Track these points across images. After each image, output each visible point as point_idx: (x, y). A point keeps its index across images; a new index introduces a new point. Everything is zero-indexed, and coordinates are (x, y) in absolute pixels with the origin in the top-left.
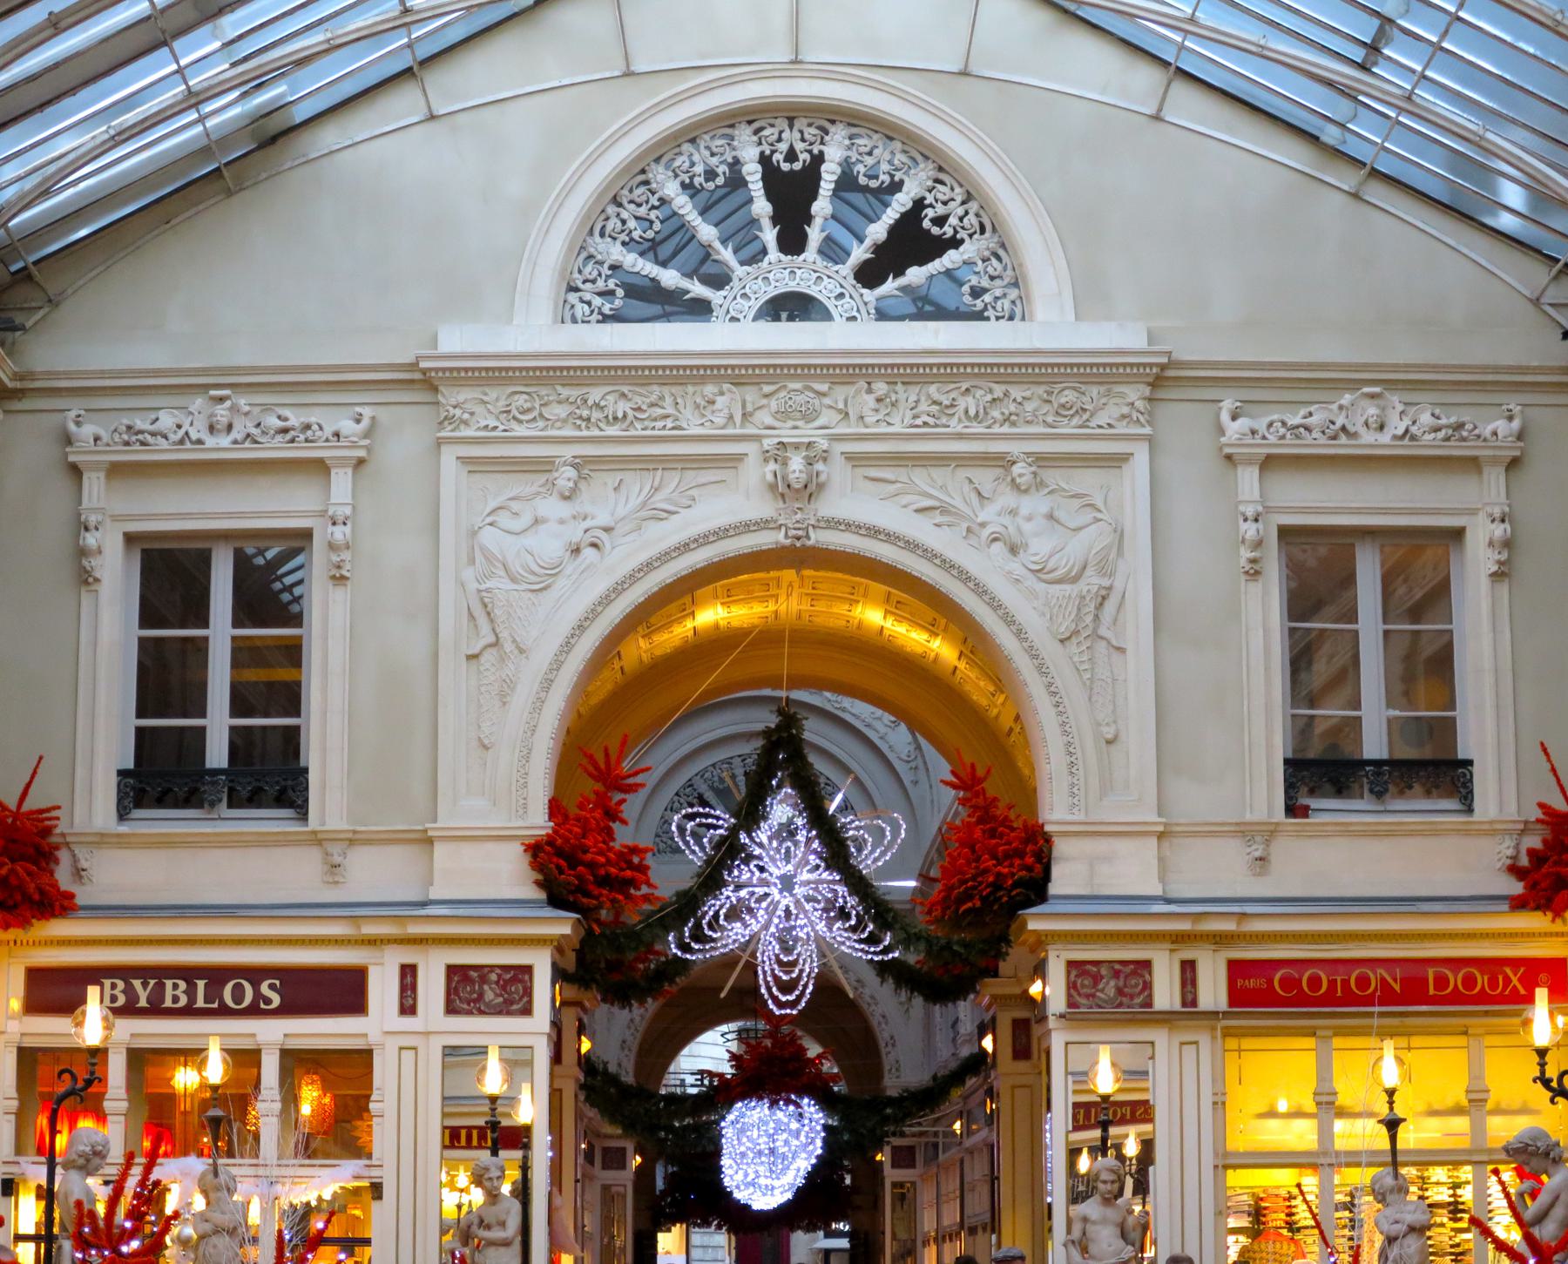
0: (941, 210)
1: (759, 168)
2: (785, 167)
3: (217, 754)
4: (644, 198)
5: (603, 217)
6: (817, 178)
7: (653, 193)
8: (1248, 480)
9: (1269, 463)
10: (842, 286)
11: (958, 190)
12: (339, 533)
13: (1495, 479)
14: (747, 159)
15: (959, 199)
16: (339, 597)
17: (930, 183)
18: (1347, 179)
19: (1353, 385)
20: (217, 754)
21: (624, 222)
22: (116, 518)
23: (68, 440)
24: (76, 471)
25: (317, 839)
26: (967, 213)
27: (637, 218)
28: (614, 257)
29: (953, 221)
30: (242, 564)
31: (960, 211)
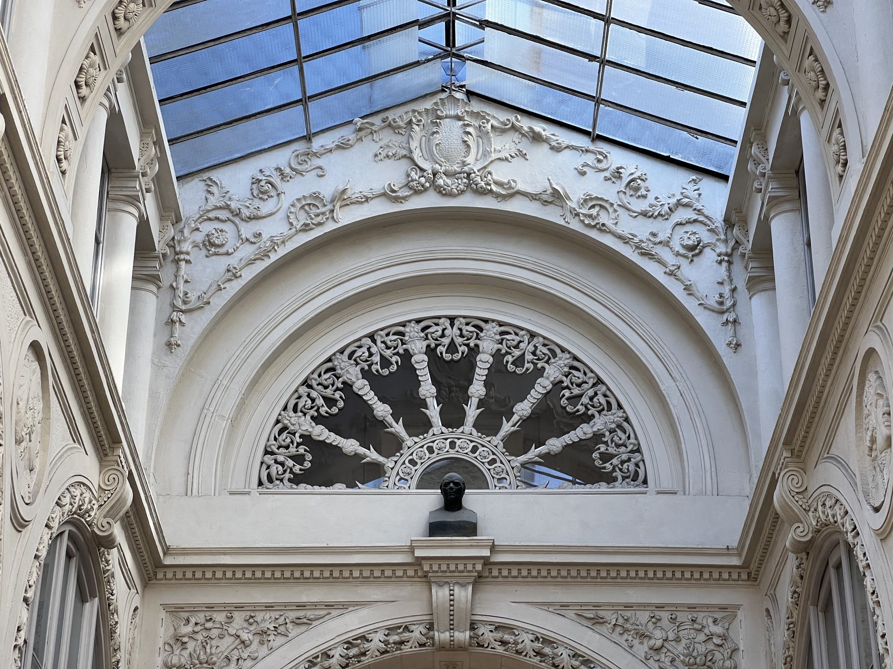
0: (576, 391)
1: (426, 358)
2: (447, 357)
4: (330, 381)
5: (296, 395)
6: (472, 366)
7: (338, 378)
10: (494, 454)
11: (590, 374)
14: (416, 351)
15: (591, 382)
17: (566, 369)
21: (313, 400)
26: (596, 394)
27: (324, 398)
28: (304, 428)
29: (585, 400)
31: (591, 393)
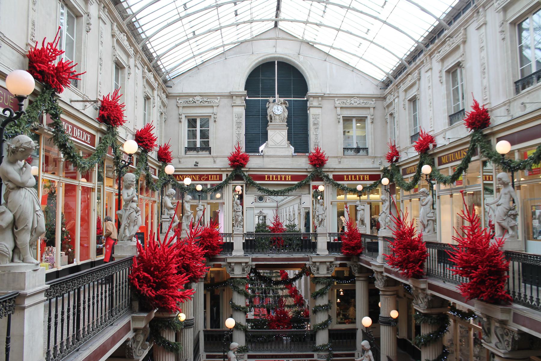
3: (198, 145)
8: (339, 109)
9: (341, 108)
12: (215, 116)
13: (372, 109)
16: (215, 124)
18: (351, 69)
19: (353, 97)
20: (198, 145)
22: (184, 114)
23: (177, 102)
24: (178, 107)
30: (201, 120)
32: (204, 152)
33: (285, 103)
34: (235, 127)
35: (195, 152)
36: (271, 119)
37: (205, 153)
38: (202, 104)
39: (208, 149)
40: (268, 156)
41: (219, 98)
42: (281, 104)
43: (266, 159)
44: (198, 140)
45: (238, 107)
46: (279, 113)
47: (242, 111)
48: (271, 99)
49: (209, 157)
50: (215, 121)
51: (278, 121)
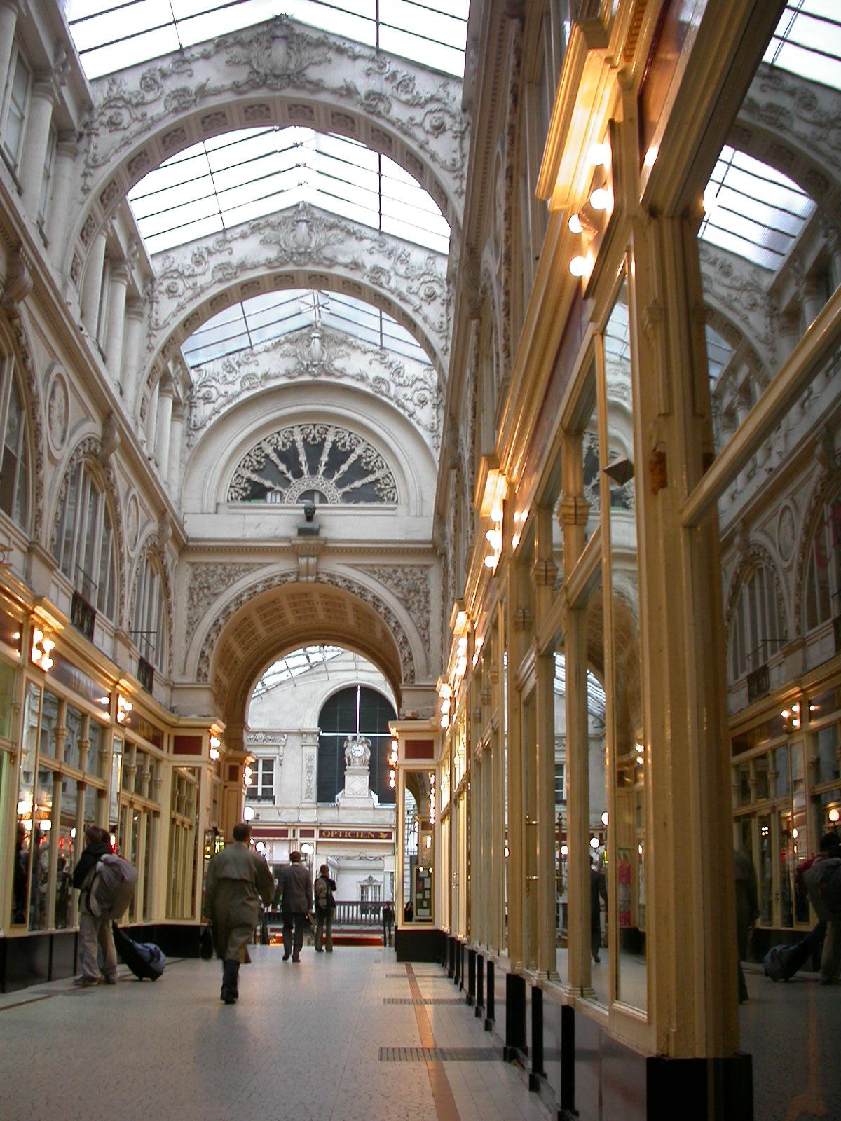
3: (260, 793)
20: (260, 793)
25: (277, 808)
32: (267, 802)
33: (367, 742)
34: (305, 772)
35: (256, 802)
36: (349, 760)
37: (268, 804)
38: (265, 743)
39: (272, 798)
40: (344, 808)
41: (285, 735)
42: (363, 742)
43: (341, 812)
44: (260, 786)
45: (309, 748)
46: (358, 754)
47: (313, 752)
48: (350, 735)
49: (272, 808)
50: (281, 764)
51: (358, 764)
